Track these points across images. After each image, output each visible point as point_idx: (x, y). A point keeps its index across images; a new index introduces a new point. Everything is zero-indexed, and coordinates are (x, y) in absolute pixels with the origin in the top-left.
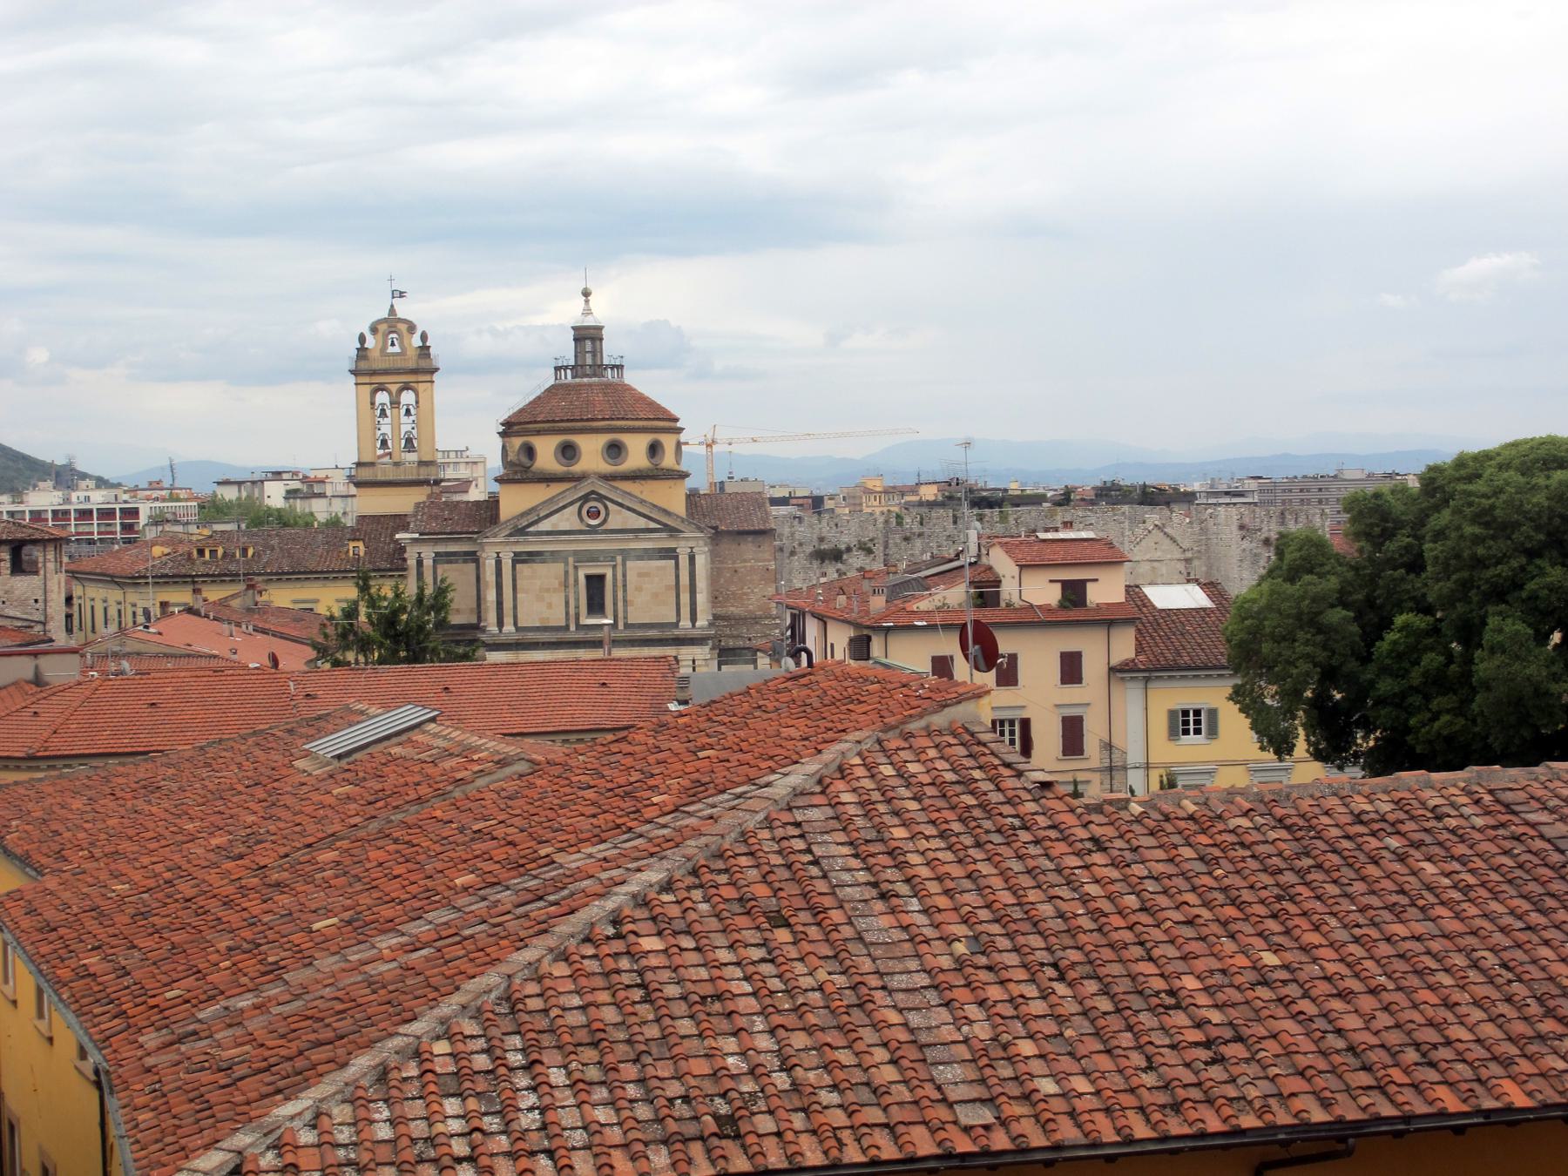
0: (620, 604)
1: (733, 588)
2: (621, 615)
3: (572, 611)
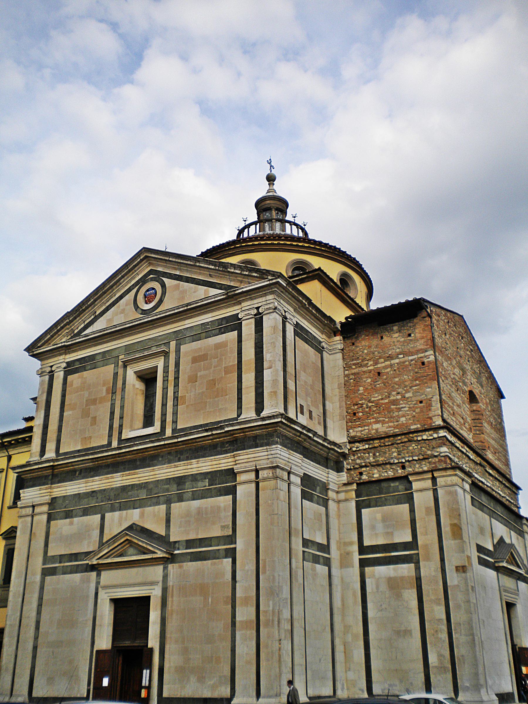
0: (170, 404)
1: (376, 397)
2: (169, 418)
3: (116, 425)
